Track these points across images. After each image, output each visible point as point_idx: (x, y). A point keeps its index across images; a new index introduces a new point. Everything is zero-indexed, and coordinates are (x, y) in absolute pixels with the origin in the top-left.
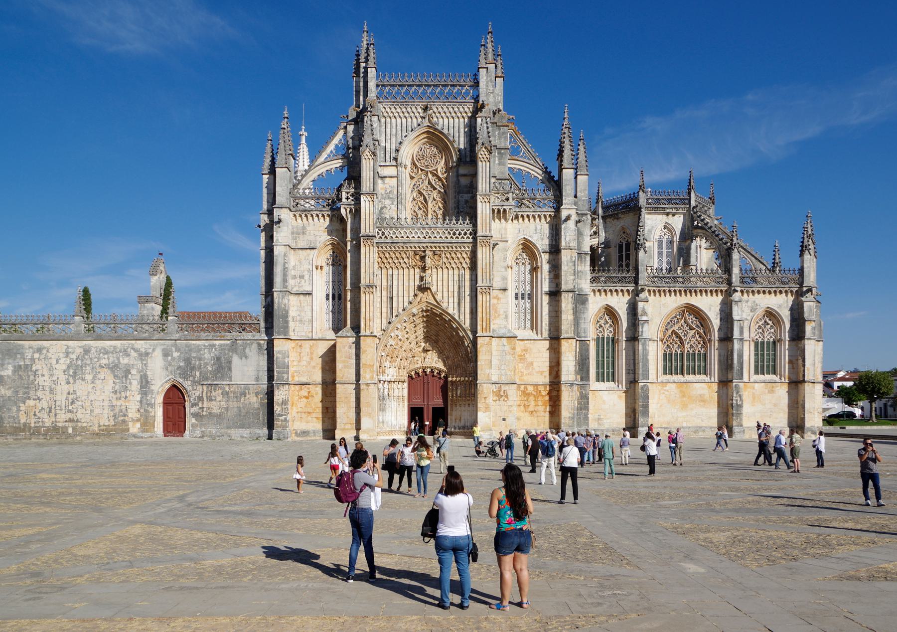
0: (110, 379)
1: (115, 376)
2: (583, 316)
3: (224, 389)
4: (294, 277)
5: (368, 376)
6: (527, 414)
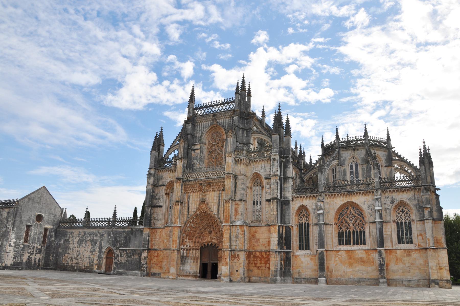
0: (90, 246)
1: (92, 245)
2: (287, 212)
3: (126, 251)
4: (156, 199)
5: (174, 246)
6: (256, 268)
